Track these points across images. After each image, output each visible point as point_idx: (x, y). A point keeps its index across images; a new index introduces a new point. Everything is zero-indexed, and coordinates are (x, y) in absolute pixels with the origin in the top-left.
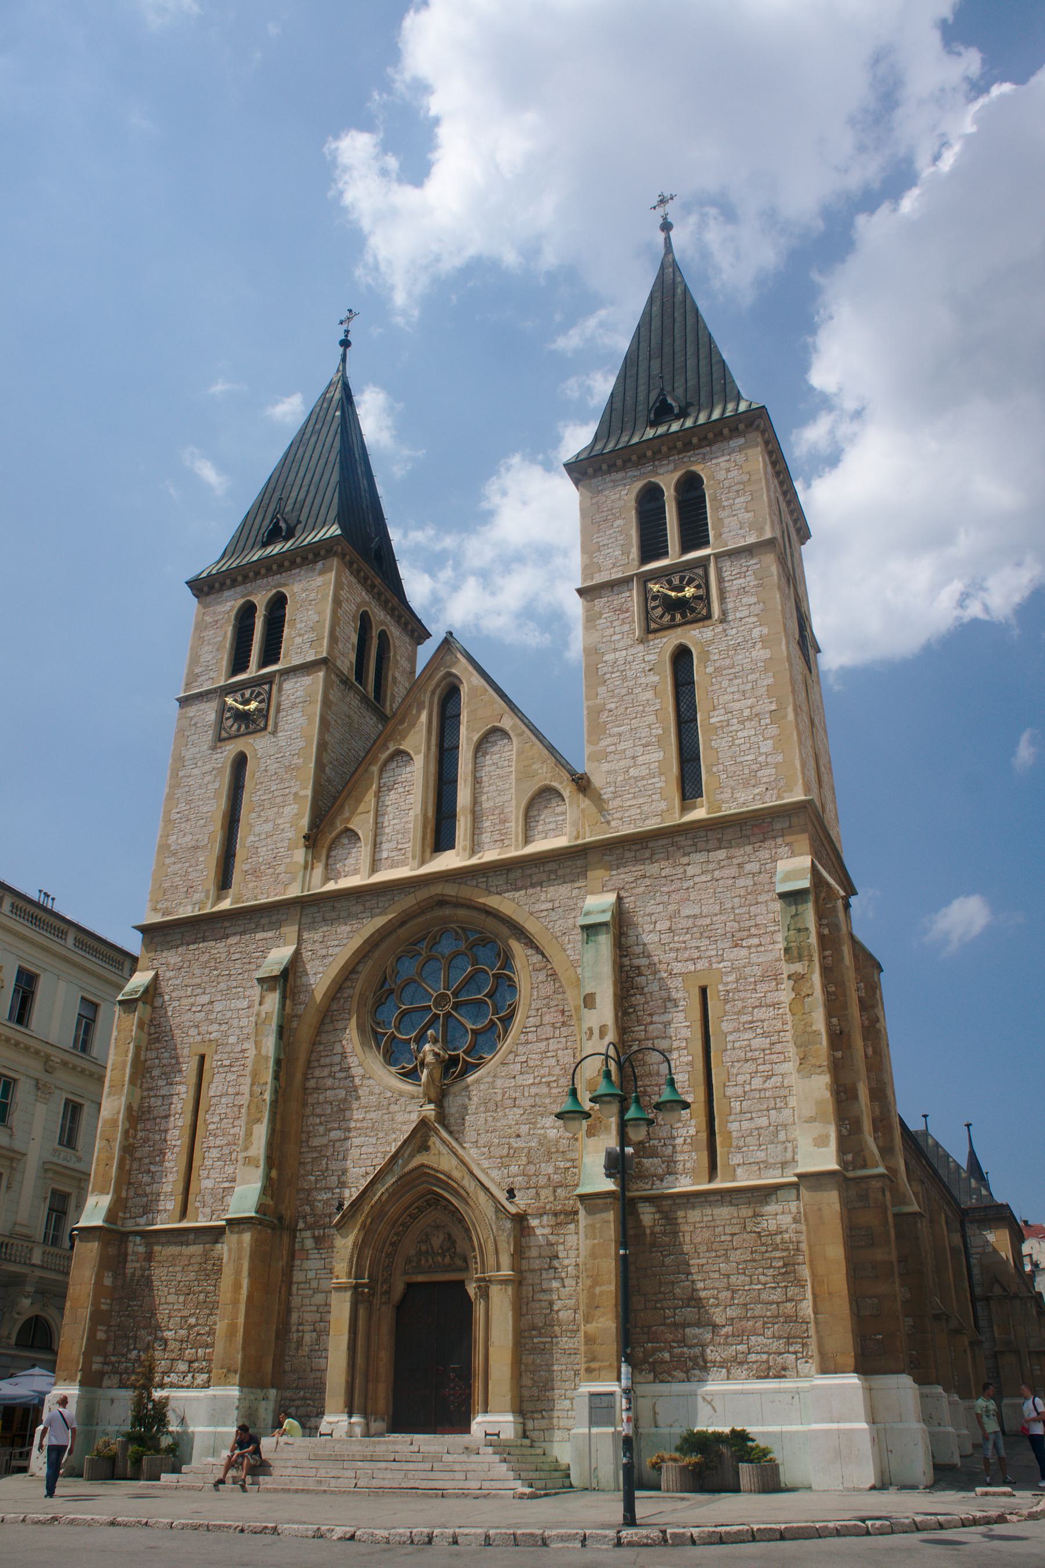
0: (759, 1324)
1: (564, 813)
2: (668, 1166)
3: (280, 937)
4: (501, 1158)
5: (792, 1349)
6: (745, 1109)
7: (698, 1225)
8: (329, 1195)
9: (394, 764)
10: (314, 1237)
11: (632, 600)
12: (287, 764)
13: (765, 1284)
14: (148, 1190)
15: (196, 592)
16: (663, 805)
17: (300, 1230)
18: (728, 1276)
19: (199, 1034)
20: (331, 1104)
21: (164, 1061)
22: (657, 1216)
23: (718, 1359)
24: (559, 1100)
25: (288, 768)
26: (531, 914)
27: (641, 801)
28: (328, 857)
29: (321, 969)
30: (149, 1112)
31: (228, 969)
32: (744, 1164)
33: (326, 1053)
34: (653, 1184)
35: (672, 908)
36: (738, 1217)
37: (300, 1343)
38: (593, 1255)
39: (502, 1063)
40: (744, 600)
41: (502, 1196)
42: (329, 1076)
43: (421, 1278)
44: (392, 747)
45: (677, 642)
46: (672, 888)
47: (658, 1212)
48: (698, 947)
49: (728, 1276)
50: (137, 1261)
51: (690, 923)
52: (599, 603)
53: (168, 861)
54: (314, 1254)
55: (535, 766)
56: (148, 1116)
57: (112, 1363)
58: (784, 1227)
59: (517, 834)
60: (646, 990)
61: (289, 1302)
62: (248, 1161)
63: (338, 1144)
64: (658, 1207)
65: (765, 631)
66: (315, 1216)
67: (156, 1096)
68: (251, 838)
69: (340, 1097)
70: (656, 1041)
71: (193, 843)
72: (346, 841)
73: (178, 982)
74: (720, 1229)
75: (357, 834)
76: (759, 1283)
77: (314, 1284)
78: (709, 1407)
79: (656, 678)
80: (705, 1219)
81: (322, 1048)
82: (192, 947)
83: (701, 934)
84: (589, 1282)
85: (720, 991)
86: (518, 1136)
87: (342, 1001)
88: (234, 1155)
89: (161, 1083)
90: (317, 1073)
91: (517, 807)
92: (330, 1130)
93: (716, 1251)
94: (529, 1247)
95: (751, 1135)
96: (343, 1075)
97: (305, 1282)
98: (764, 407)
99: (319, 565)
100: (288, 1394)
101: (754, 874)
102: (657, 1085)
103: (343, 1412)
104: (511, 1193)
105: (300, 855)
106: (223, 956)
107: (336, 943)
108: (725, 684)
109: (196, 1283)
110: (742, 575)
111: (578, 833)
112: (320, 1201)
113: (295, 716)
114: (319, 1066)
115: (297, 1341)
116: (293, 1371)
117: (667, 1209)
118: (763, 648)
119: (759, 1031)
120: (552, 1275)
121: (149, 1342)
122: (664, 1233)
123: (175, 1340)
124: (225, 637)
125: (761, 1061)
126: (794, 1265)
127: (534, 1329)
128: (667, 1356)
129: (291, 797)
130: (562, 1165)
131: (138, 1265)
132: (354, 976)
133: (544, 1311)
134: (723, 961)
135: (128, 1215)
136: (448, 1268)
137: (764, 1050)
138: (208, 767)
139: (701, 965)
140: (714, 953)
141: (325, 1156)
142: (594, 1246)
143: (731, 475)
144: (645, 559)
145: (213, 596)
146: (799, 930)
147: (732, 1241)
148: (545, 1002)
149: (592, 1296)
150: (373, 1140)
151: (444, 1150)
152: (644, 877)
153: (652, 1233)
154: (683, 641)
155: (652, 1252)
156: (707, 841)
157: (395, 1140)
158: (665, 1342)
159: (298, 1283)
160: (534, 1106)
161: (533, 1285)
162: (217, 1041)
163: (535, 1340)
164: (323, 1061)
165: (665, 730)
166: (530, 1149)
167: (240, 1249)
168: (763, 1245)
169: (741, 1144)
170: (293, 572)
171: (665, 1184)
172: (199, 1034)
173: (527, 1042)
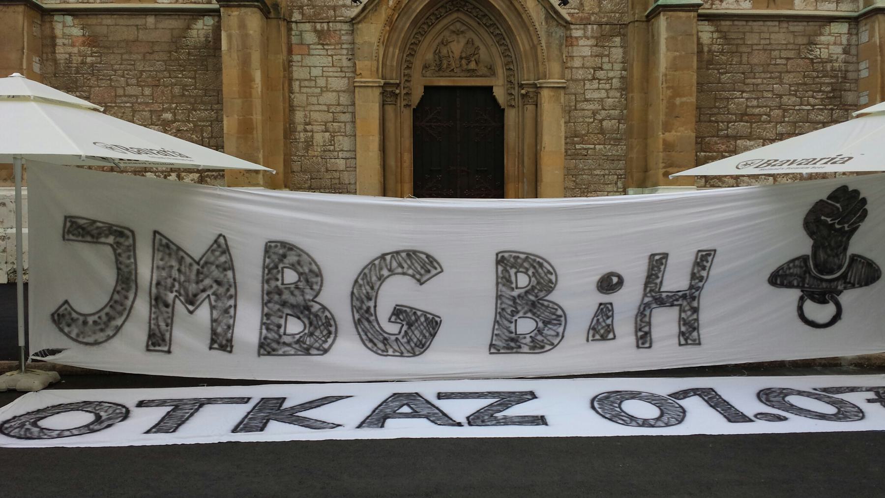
7: (755, 47)
10: (315, 31)
13: (813, 106)
17: (296, 22)
18: (780, 96)
22: (715, 35)
34: (712, 4)
36: (794, 43)
37: (309, 144)
38: (674, 66)
43: (443, 82)
47: (717, 31)
49: (780, 96)
50: (73, 45)
54: (317, 50)
58: (835, 57)
61: (290, 100)
64: (717, 26)
66: (314, 7)
74: (776, 53)
76: (809, 104)
77: (321, 82)
80: (763, 42)
84: (669, 93)
94: (572, 57)
97: (310, 80)
109: (166, 74)
116: (304, 172)
117: (725, 29)
120: (596, 86)
122: (722, 52)
126: (841, 90)
127: (576, 137)
131: (75, 50)
133: (587, 120)
136: (472, 73)
142: (675, 58)
147: (786, 65)
149: (671, 107)
153: (710, 51)
155: (708, 69)
159: (300, 80)
161: (575, 94)
163: (578, 147)
167: (245, 37)
171: (724, 4)
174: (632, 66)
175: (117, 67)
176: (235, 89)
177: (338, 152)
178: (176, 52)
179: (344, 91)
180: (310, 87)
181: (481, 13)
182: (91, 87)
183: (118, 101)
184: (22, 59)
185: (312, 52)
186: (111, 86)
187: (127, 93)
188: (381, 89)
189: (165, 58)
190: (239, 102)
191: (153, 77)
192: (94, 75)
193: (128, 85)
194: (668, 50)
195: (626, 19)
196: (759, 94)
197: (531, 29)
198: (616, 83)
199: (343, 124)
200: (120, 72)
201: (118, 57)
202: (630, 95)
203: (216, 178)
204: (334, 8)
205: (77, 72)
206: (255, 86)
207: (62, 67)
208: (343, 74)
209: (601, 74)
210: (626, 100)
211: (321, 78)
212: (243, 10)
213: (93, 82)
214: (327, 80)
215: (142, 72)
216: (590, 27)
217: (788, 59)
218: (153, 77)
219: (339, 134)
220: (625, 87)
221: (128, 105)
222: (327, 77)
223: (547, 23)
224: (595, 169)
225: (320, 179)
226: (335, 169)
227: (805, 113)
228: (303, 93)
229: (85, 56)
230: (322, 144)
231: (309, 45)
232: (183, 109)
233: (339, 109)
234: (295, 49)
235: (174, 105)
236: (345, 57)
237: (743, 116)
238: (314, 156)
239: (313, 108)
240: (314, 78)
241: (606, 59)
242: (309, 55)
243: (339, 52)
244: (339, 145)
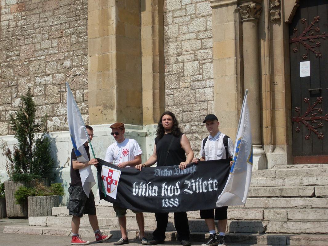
37: (180, 75)
50: (11, 13)
77: (191, 9)
109: (67, 25)
123: (53, 84)
131: (11, 16)
175: (36, 25)
176: (97, 28)
177: (206, 80)
178: (74, 4)
183: (37, 55)
186: (32, 43)
188: (236, 5)
189: (67, 11)
190: (99, 40)
192: (22, 36)
193: (43, 40)
199: (210, 50)
200: (38, 30)
206: (111, 23)
211: (190, 5)
214: (196, 7)
219: (206, 61)
221: (43, 57)
225: (190, 111)
226: (203, 99)
228: (176, 23)
229: (18, 20)
230: (191, 74)
232: (78, 55)
235: (72, 53)
238: (185, 88)
240: (184, 7)
244: (207, 73)
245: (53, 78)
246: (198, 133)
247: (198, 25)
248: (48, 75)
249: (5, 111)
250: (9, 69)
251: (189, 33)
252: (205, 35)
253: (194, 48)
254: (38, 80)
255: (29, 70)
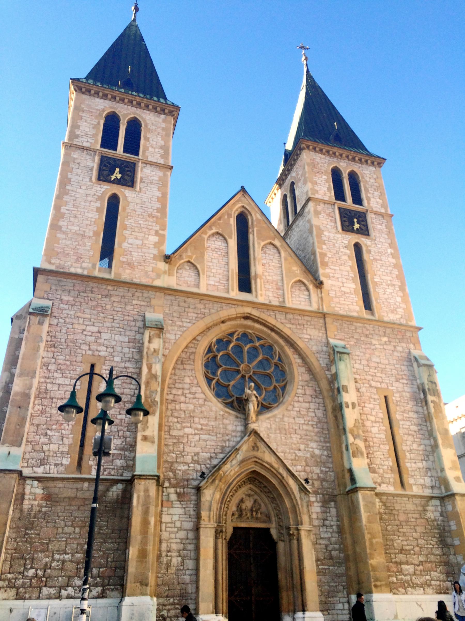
0: (434, 565)
1: (309, 295)
2: (382, 479)
3: (150, 306)
4: (292, 460)
5: (449, 579)
6: (412, 458)
7: (400, 511)
8: (186, 467)
9: (214, 239)
10: (176, 493)
11: (334, 213)
12: (149, 213)
13: (433, 545)
14: (45, 448)
15: (76, 88)
16: (357, 308)
17: (166, 488)
19: (90, 349)
20: (185, 412)
21: (60, 362)
23: (419, 583)
24: (318, 435)
25: (150, 216)
26: (300, 338)
27: (348, 303)
28: (177, 272)
29: (179, 333)
30: (46, 393)
31: (112, 315)
32: (415, 484)
33: (179, 381)
35: (367, 356)
37: (168, 565)
38: (369, 521)
39: (287, 409)
40: (383, 235)
41: (303, 482)
42: (183, 394)
43: (243, 525)
44: (214, 230)
45: (356, 241)
46: (367, 346)
47: (381, 502)
48: (381, 377)
49: (417, 539)
50: (35, 500)
51: (376, 365)
52: (319, 208)
53: (59, 235)
54: (177, 504)
55: (295, 268)
56: (45, 396)
57: (9, 580)
59: (288, 297)
60: (360, 390)
62: (145, 438)
63: (190, 437)
64: (381, 499)
65: (393, 251)
66: (176, 479)
67: (52, 383)
68: (125, 245)
69: (190, 409)
70: (368, 416)
71: (82, 233)
72: (187, 268)
73: (72, 313)
74: (410, 515)
75: (194, 266)
76: (431, 544)
78: (420, 608)
79: (348, 252)
81: (176, 377)
82: (82, 294)
83: (382, 371)
85: (393, 400)
86: (300, 450)
87: (188, 354)
88: (121, 433)
89: (56, 375)
90: (174, 391)
91: (288, 285)
92: (184, 427)
93: (410, 526)
95: (416, 470)
96: (192, 396)
97: (172, 523)
98: (386, 159)
99: (163, 116)
100: (162, 601)
101: (401, 352)
102: (371, 437)
103: (213, 613)
104: (307, 481)
105: (162, 266)
106: (108, 307)
107: (188, 321)
108: (379, 266)
110: (381, 224)
111: (319, 307)
112: (180, 470)
113: (152, 189)
114: (175, 388)
115: (167, 564)
117: (384, 501)
118: (393, 258)
119: (412, 422)
120: (325, 530)
121: (46, 564)
122: (385, 513)
123: (71, 561)
124: (99, 123)
125: (415, 436)
128: (395, 580)
129: (153, 233)
130: (324, 469)
131: (36, 503)
132: (194, 341)
134: (392, 386)
135: (26, 465)
137: (416, 432)
138: (89, 192)
139: (384, 386)
140: (388, 382)
141: (182, 443)
142: (369, 516)
143: (371, 181)
144: (337, 198)
145: (89, 97)
146: (432, 382)
147: (416, 522)
148: (306, 383)
150: (214, 438)
151: (267, 452)
152: (353, 337)
154: (359, 241)
156: (379, 331)
157: (228, 440)
158: (393, 572)
159: (166, 523)
160: (306, 435)
162: (105, 357)
163: (320, 567)
164: (177, 385)
165: (355, 276)
166: (307, 458)
167: (147, 496)
168: (429, 525)
169: (413, 474)
170: (145, 111)
172: (90, 349)
173: (299, 401)
174: (342, 519)
175: (60, 514)
179: (191, 530)
180: (172, 527)
181: (263, 486)
182: (41, 527)
183: (58, 537)
184: (9, 507)
185: (174, 506)
187: (64, 532)
190: (139, 537)
191: (82, 521)
193: (66, 526)
194: (365, 511)
195: (336, 493)
196: (407, 538)
197: (292, 496)
198: (335, 527)
200: (62, 518)
201: (62, 508)
202: (344, 536)
203: (112, 590)
204: (187, 480)
205: (35, 517)
207: (25, 514)
208: (190, 519)
209: (327, 523)
210: (341, 538)
212: (148, 480)
213: (44, 523)
215: (75, 518)
216: (318, 496)
217: (416, 518)
218: (82, 521)
220: (340, 531)
221: (64, 539)
222: (181, 521)
223: (300, 493)
224: (330, 582)
227: (430, 549)
229: (42, 507)
231: (172, 501)
233: (188, 541)
234: (165, 504)
236: (192, 509)
237: (402, 551)
239: (172, 541)
241: (328, 515)
242: (172, 507)
243: (189, 506)
245: (72, 556)
246: (178, 604)
247: (182, 534)
248: (68, 554)
249: (16, 579)
250: (26, 544)
251: (176, 538)
252: (187, 542)
253: (179, 549)
254: (57, 556)
255: (48, 547)
